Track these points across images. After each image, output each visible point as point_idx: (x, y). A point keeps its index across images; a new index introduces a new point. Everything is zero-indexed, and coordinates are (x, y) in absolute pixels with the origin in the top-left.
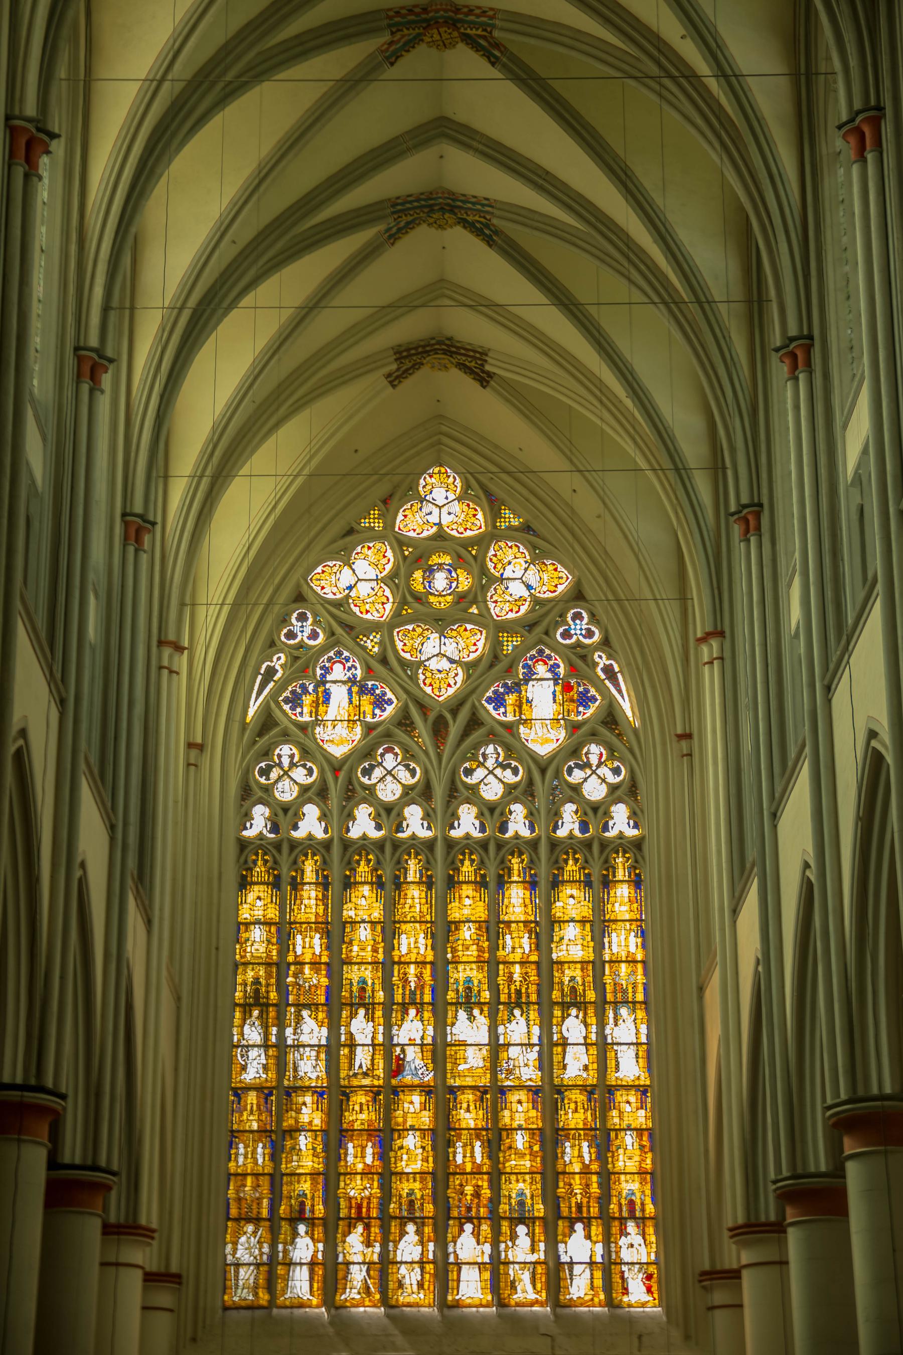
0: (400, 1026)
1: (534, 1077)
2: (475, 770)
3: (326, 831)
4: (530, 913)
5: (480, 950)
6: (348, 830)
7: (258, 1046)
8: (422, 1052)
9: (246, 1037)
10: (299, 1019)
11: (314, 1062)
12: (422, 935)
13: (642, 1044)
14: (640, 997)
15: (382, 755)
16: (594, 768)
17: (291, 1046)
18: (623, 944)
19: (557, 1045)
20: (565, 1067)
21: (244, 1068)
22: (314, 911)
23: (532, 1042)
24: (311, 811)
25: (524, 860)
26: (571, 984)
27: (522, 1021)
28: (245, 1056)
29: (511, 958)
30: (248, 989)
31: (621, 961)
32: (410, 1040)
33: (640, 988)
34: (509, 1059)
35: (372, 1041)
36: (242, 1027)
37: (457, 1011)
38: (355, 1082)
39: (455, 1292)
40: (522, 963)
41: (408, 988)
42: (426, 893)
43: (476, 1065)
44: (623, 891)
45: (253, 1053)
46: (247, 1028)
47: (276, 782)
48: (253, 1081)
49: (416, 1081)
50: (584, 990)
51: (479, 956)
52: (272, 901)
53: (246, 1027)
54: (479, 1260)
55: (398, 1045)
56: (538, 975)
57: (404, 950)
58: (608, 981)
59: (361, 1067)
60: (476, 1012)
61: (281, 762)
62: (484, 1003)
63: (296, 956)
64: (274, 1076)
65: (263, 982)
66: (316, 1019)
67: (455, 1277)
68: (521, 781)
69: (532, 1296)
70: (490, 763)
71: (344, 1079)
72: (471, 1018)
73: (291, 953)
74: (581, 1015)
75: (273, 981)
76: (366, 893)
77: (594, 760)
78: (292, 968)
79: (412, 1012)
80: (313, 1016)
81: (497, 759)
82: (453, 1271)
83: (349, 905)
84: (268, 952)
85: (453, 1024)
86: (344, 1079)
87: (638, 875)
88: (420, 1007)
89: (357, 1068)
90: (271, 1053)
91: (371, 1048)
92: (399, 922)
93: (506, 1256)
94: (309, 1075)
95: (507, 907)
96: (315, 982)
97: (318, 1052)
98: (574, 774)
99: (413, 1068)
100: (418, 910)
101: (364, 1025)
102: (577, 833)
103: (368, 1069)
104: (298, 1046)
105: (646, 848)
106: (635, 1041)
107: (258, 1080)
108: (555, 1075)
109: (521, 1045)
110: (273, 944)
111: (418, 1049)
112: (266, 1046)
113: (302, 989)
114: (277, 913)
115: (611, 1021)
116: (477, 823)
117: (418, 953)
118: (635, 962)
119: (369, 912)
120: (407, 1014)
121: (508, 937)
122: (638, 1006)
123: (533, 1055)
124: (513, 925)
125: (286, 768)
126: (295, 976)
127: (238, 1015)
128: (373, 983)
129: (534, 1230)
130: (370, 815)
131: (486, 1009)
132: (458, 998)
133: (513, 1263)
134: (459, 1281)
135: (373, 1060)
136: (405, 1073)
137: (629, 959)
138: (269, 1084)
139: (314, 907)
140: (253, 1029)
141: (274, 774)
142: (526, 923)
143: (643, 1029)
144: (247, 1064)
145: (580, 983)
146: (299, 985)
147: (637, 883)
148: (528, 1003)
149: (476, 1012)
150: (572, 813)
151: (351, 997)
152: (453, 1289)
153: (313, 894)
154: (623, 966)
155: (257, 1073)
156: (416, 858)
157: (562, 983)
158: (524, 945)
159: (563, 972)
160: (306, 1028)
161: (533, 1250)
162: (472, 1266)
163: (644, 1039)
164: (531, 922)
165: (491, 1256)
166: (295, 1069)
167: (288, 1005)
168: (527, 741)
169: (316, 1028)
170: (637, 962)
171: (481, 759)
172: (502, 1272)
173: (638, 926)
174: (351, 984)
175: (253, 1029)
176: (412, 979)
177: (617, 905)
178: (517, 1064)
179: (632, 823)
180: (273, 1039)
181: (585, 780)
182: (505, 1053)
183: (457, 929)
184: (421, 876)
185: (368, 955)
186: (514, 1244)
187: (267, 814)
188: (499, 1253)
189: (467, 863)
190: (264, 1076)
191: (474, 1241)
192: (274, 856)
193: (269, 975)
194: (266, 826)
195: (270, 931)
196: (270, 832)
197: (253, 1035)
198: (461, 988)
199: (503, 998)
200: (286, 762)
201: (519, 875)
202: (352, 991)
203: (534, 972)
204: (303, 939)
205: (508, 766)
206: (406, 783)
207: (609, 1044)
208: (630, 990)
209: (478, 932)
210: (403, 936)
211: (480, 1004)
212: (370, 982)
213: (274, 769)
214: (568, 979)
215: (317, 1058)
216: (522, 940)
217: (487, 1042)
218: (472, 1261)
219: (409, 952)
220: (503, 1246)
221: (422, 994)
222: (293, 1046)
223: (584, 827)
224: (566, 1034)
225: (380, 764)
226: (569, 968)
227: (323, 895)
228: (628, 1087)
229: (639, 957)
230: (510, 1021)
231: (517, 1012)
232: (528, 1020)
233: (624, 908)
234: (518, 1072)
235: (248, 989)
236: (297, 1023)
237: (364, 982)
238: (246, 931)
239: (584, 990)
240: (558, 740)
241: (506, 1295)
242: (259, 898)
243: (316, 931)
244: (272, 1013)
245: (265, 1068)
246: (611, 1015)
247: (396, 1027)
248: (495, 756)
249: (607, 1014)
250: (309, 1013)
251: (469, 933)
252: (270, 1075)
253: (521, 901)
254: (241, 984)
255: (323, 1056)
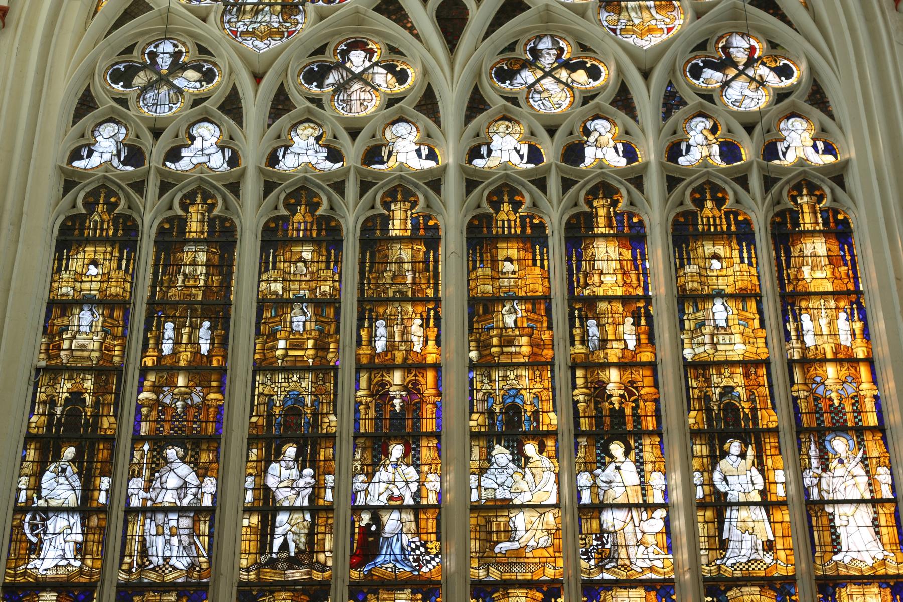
0: (370, 475)
1: (658, 564)
2: (518, 72)
3: (233, 161)
4: (635, 283)
5: (535, 344)
6: (273, 160)
7: (69, 510)
8: (417, 520)
9: (44, 493)
10: (158, 463)
11: (185, 539)
12: (419, 321)
13: (883, 501)
14: (872, 420)
15: (345, 54)
16: (741, 67)
17: (137, 511)
18: (825, 331)
19: (703, 505)
20: (724, 545)
21: (35, 549)
22: (202, 283)
23: (650, 500)
24: (208, 135)
25: (617, 201)
26: (726, 400)
27: (629, 469)
28: (39, 527)
29: (599, 356)
30: (59, 410)
31: (824, 360)
32: (391, 498)
33: (869, 405)
34: (602, 531)
35: (310, 500)
36: (38, 475)
37: (490, 448)
38: (270, 576)
40: (621, 366)
41: (388, 408)
42: (427, 253)
43: (532, 543)
44: (819, 246)
45: (57, 523)
46: (47, 479)
47: (144, 90)
48: (51, 573)
49: (405, 570)
50: (754, 410)
51: (533, 354)
52: (119, 267)
53: (47, 475)
55: (366, 508)
56: (656, 385)
57: (380, 345)
58: (802, 394)
59: (285, 546)
60: (530, 449)
61: (154, 63)
62: (548, 434)
63: (160, 357)
64: (98, 564)
65: (89, 399)
66: (194, 463)
68: (604, 88)
70: (547, 61)
71: (248, 570)
72: (520, 459)
73: (151, 352)
74: (751, 452)
75: (111, 398)
76: (307, 256)
77: (741, 57)
78: (152, 377)
79: (397, 451)
80: (188, 458)
81: (559, 56)
83: (273, 274)
84: (105, 349)
85: (482, 471)
86: (248, 570)
87: (846, 222)
88: (412, 442)
89: (276, 549)
90: (94, 521)
91: (308, 517)
92: (371, 301)
94: (173, 561)
95: (586, 275)
96: (197, 400)
97: (196, 521)
98: (704, 76)
99: (397, 551)
100: (410, 280)
101: (295, 472)
102: (717, 160)
103: (299, 552)
104: (155, 510)
105: (854, 180)
106: (868, 496)
107: (62, 571)
108: (704, 560)
109: (629, 506)
110: (115, 338)
111: (409, 516)
112: (85, 509)
113: (169, 413)
114: (128, 286)
115: (815, 462)
116: (524, 150)
117: (409, 351)
118: (853, 361)
119: (313, 285)
120: (387, 454)
121: (592, 322)
122: (868, 437)
123: (655, 523)
124: (602, 305)
125: (164, 70)
126: (156, 389)
127: (31, 454)
128: (316, 403)
130: (318, 139)
131: (550, 443)
132: (492, 425)
135: (310, 535)
136: (380, 559)
137: (840, 356)
138: (84, 579)
139: (202, 278)
140: (62, 480)
141: (141, 80)
142: (625, 300)
143: (883, 476)
144: (41, 542)
145: (744, 397)
146: (164, 406)
147: (840, 232)
148: (639, 434)
149: (530, 449)
150: (705, 132)
151: (270, 424)
153: (202, 258)
154: (831, 370)
155: (63, 557)
156: (404, 200)
157: (708, 398)
158: (626, 337)
159: (708, 380)
160: (172, 481)
163: (887, 493)
164: (638, 298)
166: (144, 553)
167: (138, 439)
168: (614, 31)
169: (192, 479)
170: (858, 361)
171: (529, 57)
173: (852, 303)
174: (271, 403)
175: (62, 480)
176: (394, 390)
177: (806, 270)
178: (620, 541)
179: (821, 146)
180: (103, 498)
181: (726, 84)
182: (595, 524)
183: (486, 311)
184: (416, 228)
185: (308, 353)
187: (122, 137)
189: (506, 207)
190: (78, 564)
192: (128, 197)
193: (100, 390)
194: (119, 154)
195: (111, 316)
196: (125, 163)
197: (60, 489)
198: (497, 409)
199: (585, 424)
200: (164, 62)
201: (609, 225)
202: (270, 416)
203: (648, 381)
204: (177, 329)
205: (581, 65)
206: (388, 91)
207: (814, 502)
208: (848, 408)
209: (531, 315)
210: (381, 323)
211: (540, 438)
212: (308, 400)
213: (142, 74)
214: (718, 391)
215: (194, 532)
216: (620, 328)
217: (553, 500)
219: (391, 346)
221: (418, 419)
222: (143, 510)
223: (730, 151)
224: (722, 487)
225: (340, 66)
226: (720, 374)
227: (221, 258)
228: (863, 580)
229: (861, 353)
230: (603, 465)
231: (617, 449)
232: (640, 464)
233: (818, 274)
234: (623, 554)
235: (59, 410)
236: (153, 471)
237: (299, 399)
238: (63, 314)
239: (754, 410)
240: (669, 30)
242: (94, 262)
243: (204, 317)
244: (103, 453)
245: (81, 550)
246: (813, 452)
247: (362, 477)
248: (554, 52)
249: (804, 450)
250: (181, 452)
251: (514, 317)
252: (89, 562)
253: (614, 265)
254: (44, 403)
255: (204, 528)
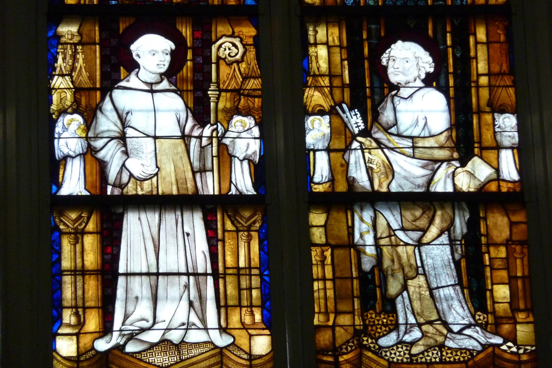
39: (93, 323)
54: (210, 186)
67: (91, 259)
69: (474, 340)
82: (78, 235)
93: (341, 168)
129: (465, 62)
133: (375, 199)
134: (108, 273)
152: (81, 309)
161: (465, 141)
162: (170, 218)
165: (260, 170)
172: (318, 235)
186: (372, 117)
188: (302, 156)
191: (171, 108)
218: (168, 186)
220: (317, 130)
241: (342, 335)
